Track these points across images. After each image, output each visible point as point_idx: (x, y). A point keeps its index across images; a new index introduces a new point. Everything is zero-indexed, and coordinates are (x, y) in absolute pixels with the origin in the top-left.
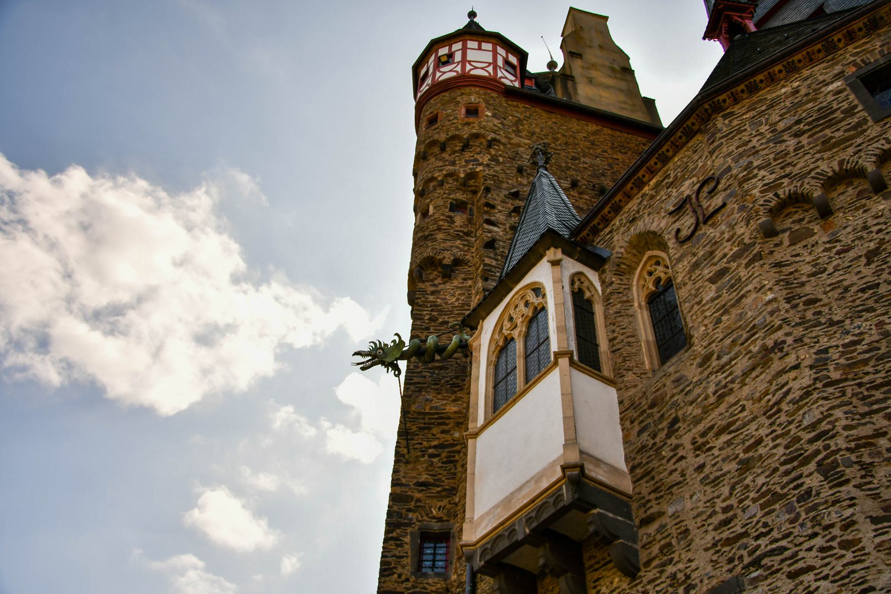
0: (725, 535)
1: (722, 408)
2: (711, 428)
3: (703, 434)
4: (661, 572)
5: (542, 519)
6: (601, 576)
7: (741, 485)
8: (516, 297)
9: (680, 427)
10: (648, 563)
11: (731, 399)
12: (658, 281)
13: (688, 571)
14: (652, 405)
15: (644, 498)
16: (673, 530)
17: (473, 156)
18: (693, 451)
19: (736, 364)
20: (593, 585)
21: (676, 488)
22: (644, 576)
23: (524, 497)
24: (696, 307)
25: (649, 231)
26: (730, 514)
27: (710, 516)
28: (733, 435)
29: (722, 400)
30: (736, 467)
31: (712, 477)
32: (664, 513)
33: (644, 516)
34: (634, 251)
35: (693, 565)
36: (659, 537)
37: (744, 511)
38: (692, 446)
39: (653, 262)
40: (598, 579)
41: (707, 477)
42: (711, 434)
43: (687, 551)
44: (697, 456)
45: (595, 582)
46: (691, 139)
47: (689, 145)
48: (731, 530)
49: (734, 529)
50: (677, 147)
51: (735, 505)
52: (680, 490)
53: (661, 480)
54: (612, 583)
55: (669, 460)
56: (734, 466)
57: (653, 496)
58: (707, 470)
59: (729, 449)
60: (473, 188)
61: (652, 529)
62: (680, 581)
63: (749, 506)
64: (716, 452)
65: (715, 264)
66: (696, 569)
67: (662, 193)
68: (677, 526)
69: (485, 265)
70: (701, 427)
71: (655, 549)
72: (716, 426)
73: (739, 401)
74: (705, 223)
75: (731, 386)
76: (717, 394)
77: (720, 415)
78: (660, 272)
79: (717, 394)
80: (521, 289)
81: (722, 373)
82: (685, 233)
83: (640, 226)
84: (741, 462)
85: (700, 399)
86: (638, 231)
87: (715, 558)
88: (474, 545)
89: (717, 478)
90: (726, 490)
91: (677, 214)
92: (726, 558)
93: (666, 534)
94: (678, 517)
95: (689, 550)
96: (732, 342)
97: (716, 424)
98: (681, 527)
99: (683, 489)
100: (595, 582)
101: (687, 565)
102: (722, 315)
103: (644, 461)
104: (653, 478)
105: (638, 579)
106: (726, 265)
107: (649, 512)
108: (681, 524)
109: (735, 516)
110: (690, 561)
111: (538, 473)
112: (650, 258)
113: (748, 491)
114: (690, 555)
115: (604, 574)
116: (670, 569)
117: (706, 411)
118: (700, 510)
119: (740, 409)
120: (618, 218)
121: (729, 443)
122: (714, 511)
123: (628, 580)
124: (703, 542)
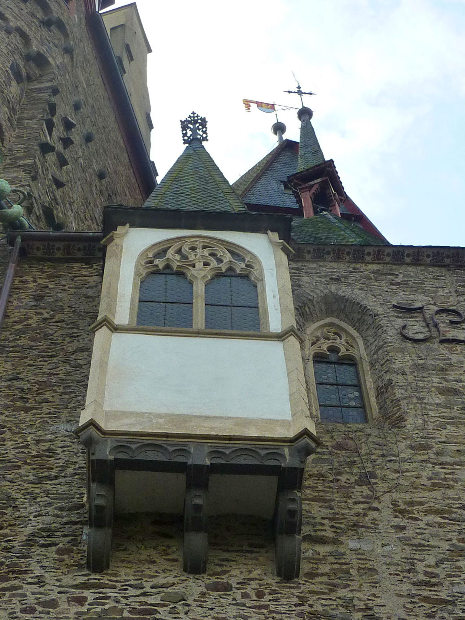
0: (426, 593)
1: (438, 494)
2: (421, 503)
3: (411, 503)
4: (331, 590)
5: (234, 462)
6: (232, 559)
7: (451, 563)
8: (197, 239)
9: (376, 483)
10: (312, 575)
11: (451, 493)
12: (334, 350)
13: (371, 604)
14: (339, 447)
15: (314, 518)
16: (355, 562)
17: (49, 43)
18: (392, 510)
19: (459, 469)
20: (216, 562)
21: (363, 529)
22: (304, 584)
23: (212, 428)
24: (415, 400)
25: (358, 304)
26: (433, 580)
27: (409, 571)
28: (447, 521)
29: (437, 488)
30: (448, 548)
31: (415, 541)
32: (342, 543)
33: (313, 534)
34: (323, 307)
35: (378, 601)
36: (331, 559)
37: (452, 584)
38: (392, 506)
39: (333, 330)
40: (228, 560)
41: (409, 539)
42: (420, 508)
43: (373, 587)
44: (396, 517)
45: (222, 560)
46: (434, 266)
47: (431, 269)
48: (433, 593)
49: (438, 594)
50: (418, 260)
51: (442, 576)
52: (369, 534)
53: (343, 514)
54: (250, 572)
55: (356, 503)
56: (446, 546)
57: (326, 522)
58: (409, 533)
59: (441, 530)
60: (30, 71)
61: (323, 549)
62: (357, 608)
63: (460, 583)
64: (422, 525)
65: (447, 381)
66: (382, 606)
67: (383, 283)
68: (360, 561)
69: (35, 163)
70: (407, 497)
71: (325, 568)
72: (427, 505)
73: (459, 499)
74: (442, 342)
75: (452, 483)
76: (433, 481)
77: (433, 498)
78: (341, 343)
79: (433, 481)
80: (210, 238)
81: (442, 468)
82: (410, 333)
83: (344, 291)
84: (453, 545)
85: (407, 474)
86: (340, 293)
87: (409, 606)
88: (104, 433)
89: (420, 545)
90: (432, 561)
91: (401, 312)
92: (425, 612)
93: (343, 561)
94: (363, 554)
95: (376, 587)
96: (458, 451)
97: (427, 503)
98: (366, 563)
99: (372, 535)
100: (222, 560)
101: (369, 598)
102: (448, 423)
103: (320, 488)
104: (331, 508)
105: (295, 583)
106: (460, 389)
107: (319, 533)
108: (366, 562)
109: (441, 584)
110: (374, 595)
111: (246, 419)
112: (331, 325)
113: (461, 572)
114: (374, 591)
115: (238, 558)
116: (342, 593)
117: (415, 487)
118: (395, 561)
119: (458, 506)
120: (313, 265)
121: (441, 525)
122: (414, 569)
123: (278, 579)
124: (393, 587)
